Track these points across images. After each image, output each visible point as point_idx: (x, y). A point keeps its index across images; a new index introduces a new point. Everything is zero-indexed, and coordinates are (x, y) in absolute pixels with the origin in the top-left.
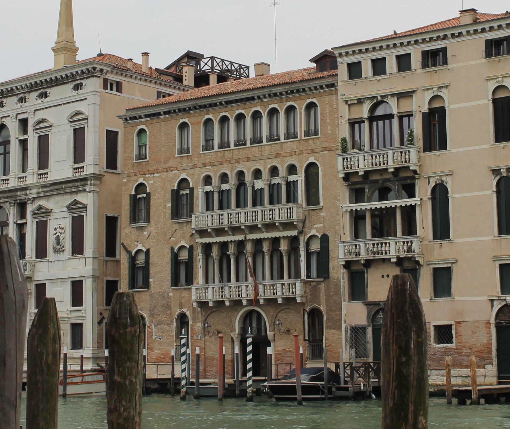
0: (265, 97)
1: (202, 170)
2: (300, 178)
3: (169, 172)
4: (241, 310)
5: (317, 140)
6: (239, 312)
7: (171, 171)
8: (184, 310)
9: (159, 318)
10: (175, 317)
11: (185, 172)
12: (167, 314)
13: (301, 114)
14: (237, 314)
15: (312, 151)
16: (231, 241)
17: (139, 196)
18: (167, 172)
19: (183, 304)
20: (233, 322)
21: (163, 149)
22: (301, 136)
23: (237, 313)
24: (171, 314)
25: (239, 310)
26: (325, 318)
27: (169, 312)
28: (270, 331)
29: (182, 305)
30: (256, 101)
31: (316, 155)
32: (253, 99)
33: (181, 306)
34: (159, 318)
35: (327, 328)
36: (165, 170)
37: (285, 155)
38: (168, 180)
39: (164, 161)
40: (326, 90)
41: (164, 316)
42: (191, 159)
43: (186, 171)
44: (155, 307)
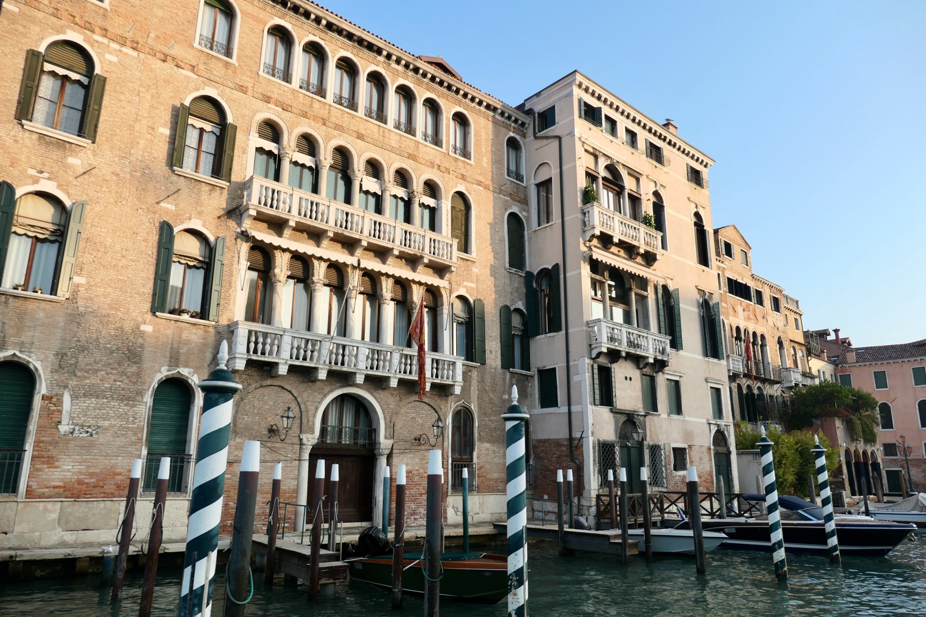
0: (398, 62)
1: (260, 104)
2: (446, 207)
3: (169, 65)
4: (331, 391)
5: (468, 167)
6: (325, 396)
7: (177, 66)
8: (185, 372)
9: (93, 380)
10: (155, 384)
11: (217, 88)
12: (123, 373)
13: (448, 119)
14: (322, 399)
15: (463, 177)
16: (320, 259)
17: (48, 67)
18: (164, 61)
19: (182, 358)
20: (310, 413)
21: (160, 13)
22: (448, 149)
23: (321, 396)
24: (138, 374)
25: (326, 391)
26: (476, 424)
27: (134, 369)
28: (386, 438)
29: (177, 359)
30: (379, 58)
31: (469, 185)
32: (379, 51)
33: (175, 360)
34: (93, 380)
35: (481, 440)
36: (162, 57)
37: (423, 162)
38: (167, 82)
39: (158, 37)
40: (482, 109)
41: (113, 377)
42: (234, 72)
43: (221, 88)
44: (84, 349)
